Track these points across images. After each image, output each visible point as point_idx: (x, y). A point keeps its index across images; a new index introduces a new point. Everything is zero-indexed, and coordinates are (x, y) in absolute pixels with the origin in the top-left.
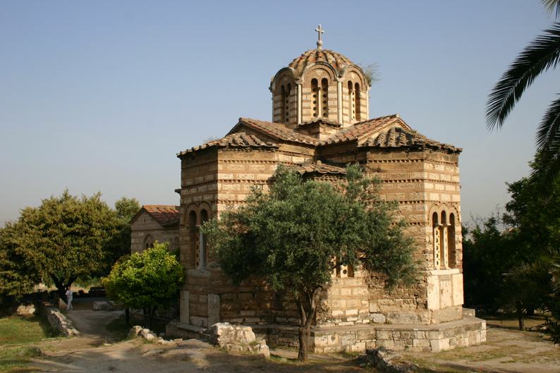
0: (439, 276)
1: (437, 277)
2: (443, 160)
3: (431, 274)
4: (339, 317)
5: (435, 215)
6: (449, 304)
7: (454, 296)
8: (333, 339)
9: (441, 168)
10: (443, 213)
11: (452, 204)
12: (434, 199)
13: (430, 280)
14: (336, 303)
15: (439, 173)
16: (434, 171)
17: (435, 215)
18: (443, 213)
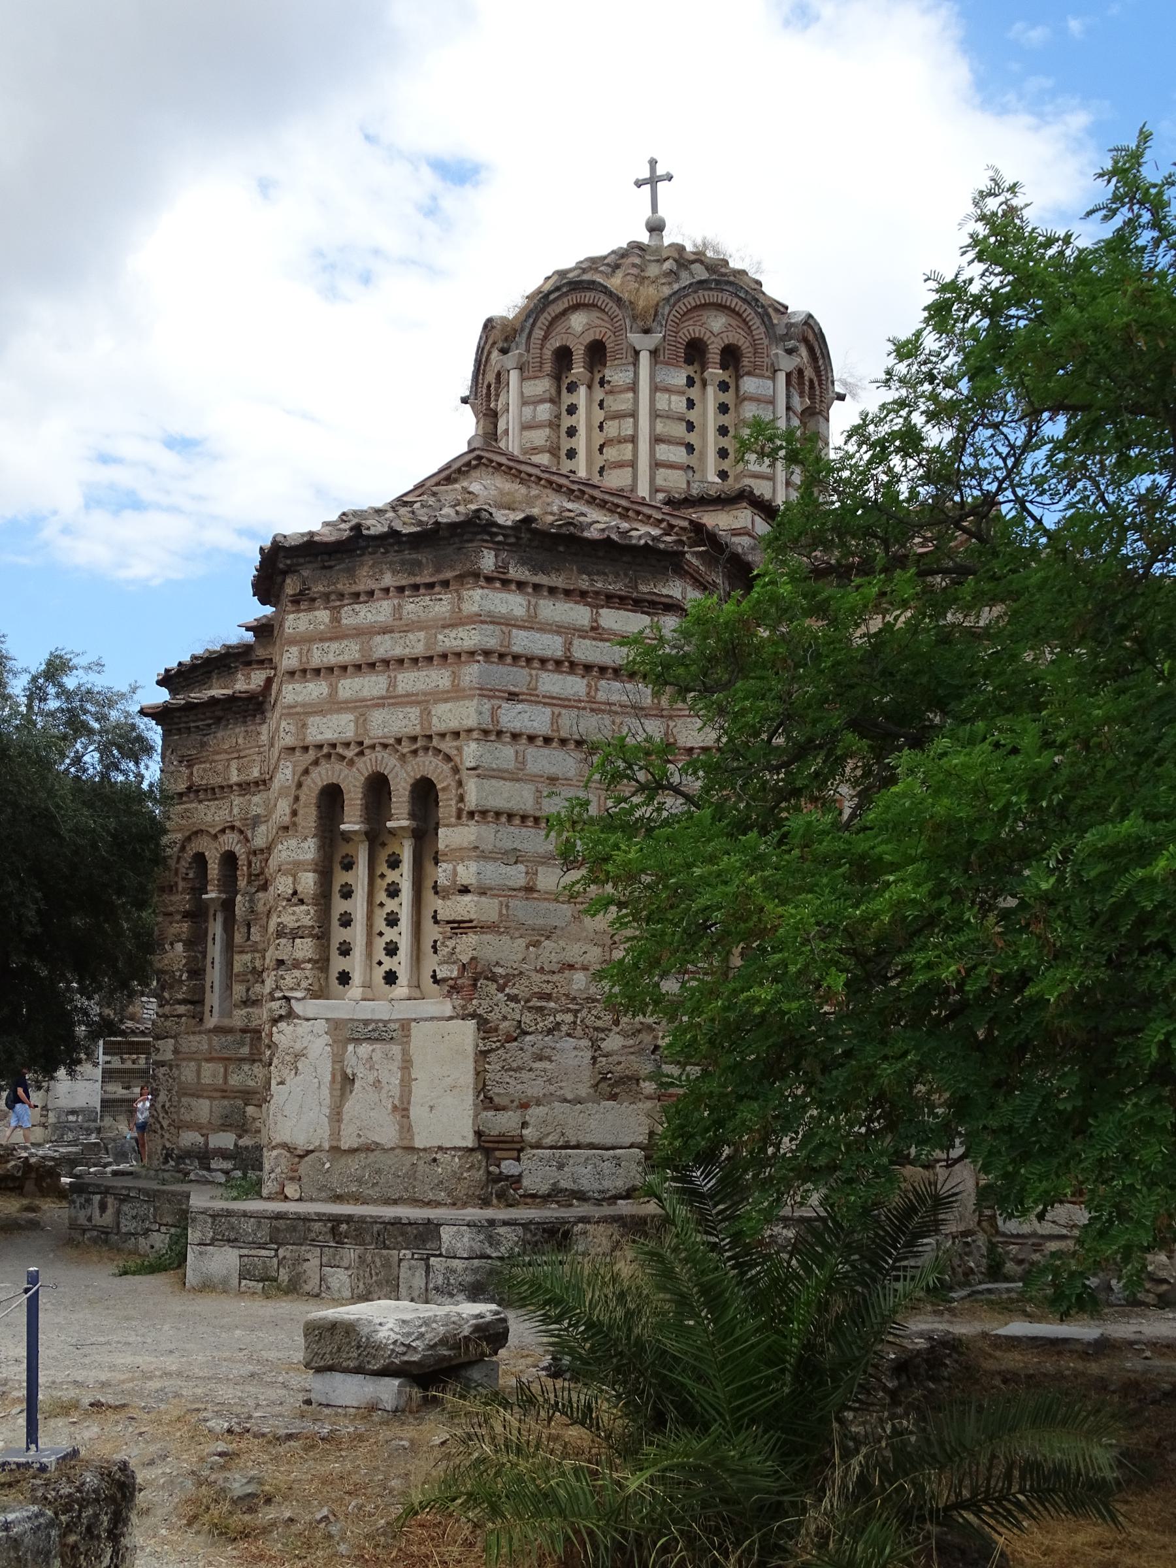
0: (336, 1025)
1: (321, 1026)
2: (388, 580)
3: (290, 1015)
4: (187, 1154)
5: (332, 797)
6: (387, 1133)
7: (414, 1112)
8: (103, 1207)
9: (380, 612)
10: (378, 786)
11: (423, 742)
12: (329, 735)
13: (284, 1034)
14: (189, 1108)
15: (363, 633)
16: (337, 634)
17: (332, 797)
18: (378, 786)
